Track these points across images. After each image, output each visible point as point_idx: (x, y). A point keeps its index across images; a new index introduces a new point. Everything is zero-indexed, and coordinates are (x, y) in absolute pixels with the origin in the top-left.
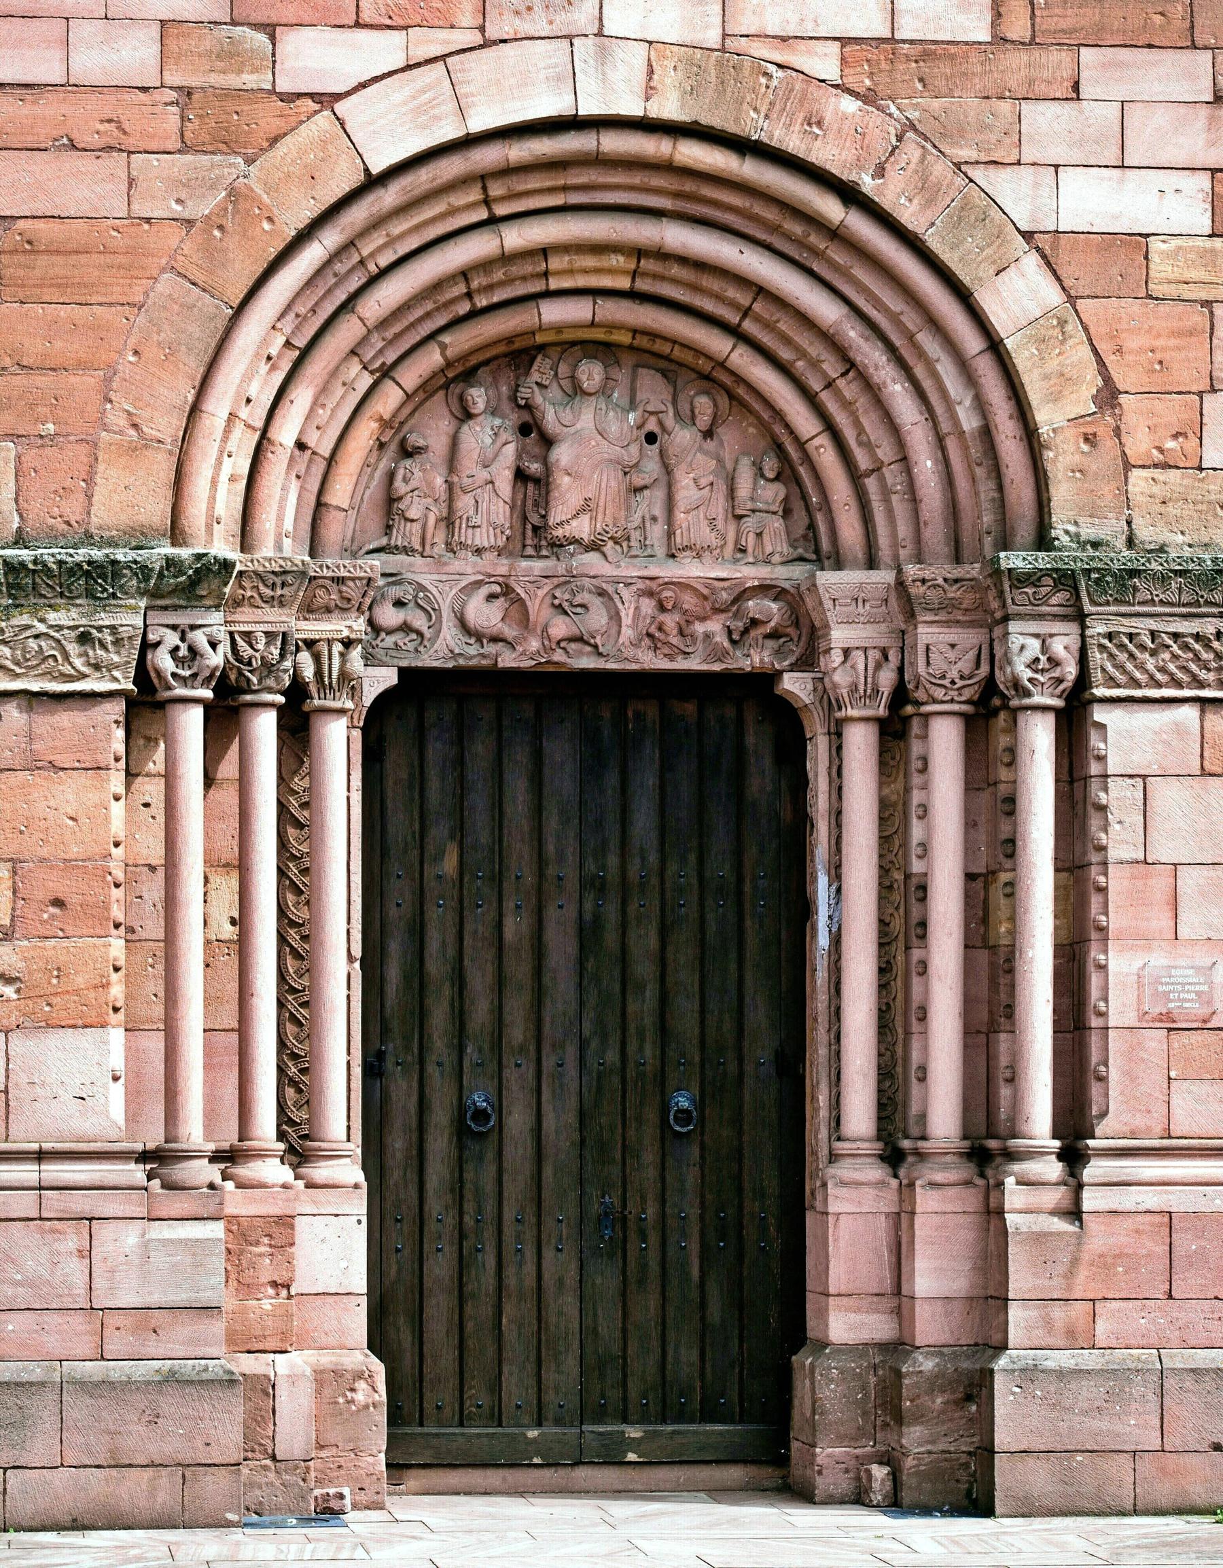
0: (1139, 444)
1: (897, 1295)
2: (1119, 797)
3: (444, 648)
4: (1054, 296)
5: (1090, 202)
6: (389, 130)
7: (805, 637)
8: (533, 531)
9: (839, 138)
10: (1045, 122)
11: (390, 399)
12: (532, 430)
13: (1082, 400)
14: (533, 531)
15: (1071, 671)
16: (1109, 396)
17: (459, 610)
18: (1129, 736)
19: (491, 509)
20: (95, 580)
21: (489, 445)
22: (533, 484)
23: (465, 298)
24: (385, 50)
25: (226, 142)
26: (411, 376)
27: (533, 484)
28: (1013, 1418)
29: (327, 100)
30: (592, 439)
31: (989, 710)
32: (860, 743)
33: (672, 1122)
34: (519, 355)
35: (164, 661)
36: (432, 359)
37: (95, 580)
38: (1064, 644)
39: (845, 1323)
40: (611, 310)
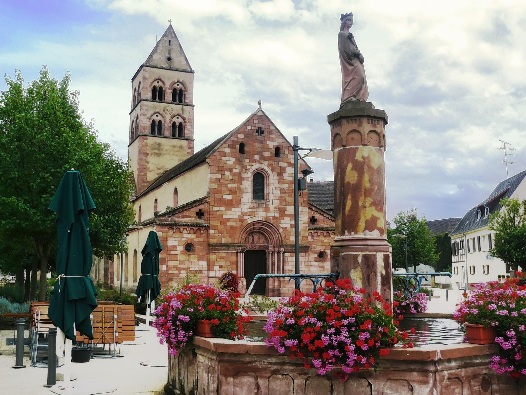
1: (274, 285)
2: (286, 258)
3: (248, 249)
5: (284, 226)
6: (250, 221)
7: (267, 248)
8: (253, 242)
9: (272, 221)
12: (253, 237)
14: (253, 242)
17: (249, 246)
18: (287, 254)
19: (251, 241)
20: (235, 246)
21: (251, 237)
22: (253, 240)
23: (250, 230)
24: (249, 217)
25: (241, 222)
27: (253, 240)
28: (282, 291)
30: (256, 237)
31: (279, 253)
32: (270, 255)
33: (257, 276)
34: (252, 233)
37: (235, 246)
39: (271, 287)
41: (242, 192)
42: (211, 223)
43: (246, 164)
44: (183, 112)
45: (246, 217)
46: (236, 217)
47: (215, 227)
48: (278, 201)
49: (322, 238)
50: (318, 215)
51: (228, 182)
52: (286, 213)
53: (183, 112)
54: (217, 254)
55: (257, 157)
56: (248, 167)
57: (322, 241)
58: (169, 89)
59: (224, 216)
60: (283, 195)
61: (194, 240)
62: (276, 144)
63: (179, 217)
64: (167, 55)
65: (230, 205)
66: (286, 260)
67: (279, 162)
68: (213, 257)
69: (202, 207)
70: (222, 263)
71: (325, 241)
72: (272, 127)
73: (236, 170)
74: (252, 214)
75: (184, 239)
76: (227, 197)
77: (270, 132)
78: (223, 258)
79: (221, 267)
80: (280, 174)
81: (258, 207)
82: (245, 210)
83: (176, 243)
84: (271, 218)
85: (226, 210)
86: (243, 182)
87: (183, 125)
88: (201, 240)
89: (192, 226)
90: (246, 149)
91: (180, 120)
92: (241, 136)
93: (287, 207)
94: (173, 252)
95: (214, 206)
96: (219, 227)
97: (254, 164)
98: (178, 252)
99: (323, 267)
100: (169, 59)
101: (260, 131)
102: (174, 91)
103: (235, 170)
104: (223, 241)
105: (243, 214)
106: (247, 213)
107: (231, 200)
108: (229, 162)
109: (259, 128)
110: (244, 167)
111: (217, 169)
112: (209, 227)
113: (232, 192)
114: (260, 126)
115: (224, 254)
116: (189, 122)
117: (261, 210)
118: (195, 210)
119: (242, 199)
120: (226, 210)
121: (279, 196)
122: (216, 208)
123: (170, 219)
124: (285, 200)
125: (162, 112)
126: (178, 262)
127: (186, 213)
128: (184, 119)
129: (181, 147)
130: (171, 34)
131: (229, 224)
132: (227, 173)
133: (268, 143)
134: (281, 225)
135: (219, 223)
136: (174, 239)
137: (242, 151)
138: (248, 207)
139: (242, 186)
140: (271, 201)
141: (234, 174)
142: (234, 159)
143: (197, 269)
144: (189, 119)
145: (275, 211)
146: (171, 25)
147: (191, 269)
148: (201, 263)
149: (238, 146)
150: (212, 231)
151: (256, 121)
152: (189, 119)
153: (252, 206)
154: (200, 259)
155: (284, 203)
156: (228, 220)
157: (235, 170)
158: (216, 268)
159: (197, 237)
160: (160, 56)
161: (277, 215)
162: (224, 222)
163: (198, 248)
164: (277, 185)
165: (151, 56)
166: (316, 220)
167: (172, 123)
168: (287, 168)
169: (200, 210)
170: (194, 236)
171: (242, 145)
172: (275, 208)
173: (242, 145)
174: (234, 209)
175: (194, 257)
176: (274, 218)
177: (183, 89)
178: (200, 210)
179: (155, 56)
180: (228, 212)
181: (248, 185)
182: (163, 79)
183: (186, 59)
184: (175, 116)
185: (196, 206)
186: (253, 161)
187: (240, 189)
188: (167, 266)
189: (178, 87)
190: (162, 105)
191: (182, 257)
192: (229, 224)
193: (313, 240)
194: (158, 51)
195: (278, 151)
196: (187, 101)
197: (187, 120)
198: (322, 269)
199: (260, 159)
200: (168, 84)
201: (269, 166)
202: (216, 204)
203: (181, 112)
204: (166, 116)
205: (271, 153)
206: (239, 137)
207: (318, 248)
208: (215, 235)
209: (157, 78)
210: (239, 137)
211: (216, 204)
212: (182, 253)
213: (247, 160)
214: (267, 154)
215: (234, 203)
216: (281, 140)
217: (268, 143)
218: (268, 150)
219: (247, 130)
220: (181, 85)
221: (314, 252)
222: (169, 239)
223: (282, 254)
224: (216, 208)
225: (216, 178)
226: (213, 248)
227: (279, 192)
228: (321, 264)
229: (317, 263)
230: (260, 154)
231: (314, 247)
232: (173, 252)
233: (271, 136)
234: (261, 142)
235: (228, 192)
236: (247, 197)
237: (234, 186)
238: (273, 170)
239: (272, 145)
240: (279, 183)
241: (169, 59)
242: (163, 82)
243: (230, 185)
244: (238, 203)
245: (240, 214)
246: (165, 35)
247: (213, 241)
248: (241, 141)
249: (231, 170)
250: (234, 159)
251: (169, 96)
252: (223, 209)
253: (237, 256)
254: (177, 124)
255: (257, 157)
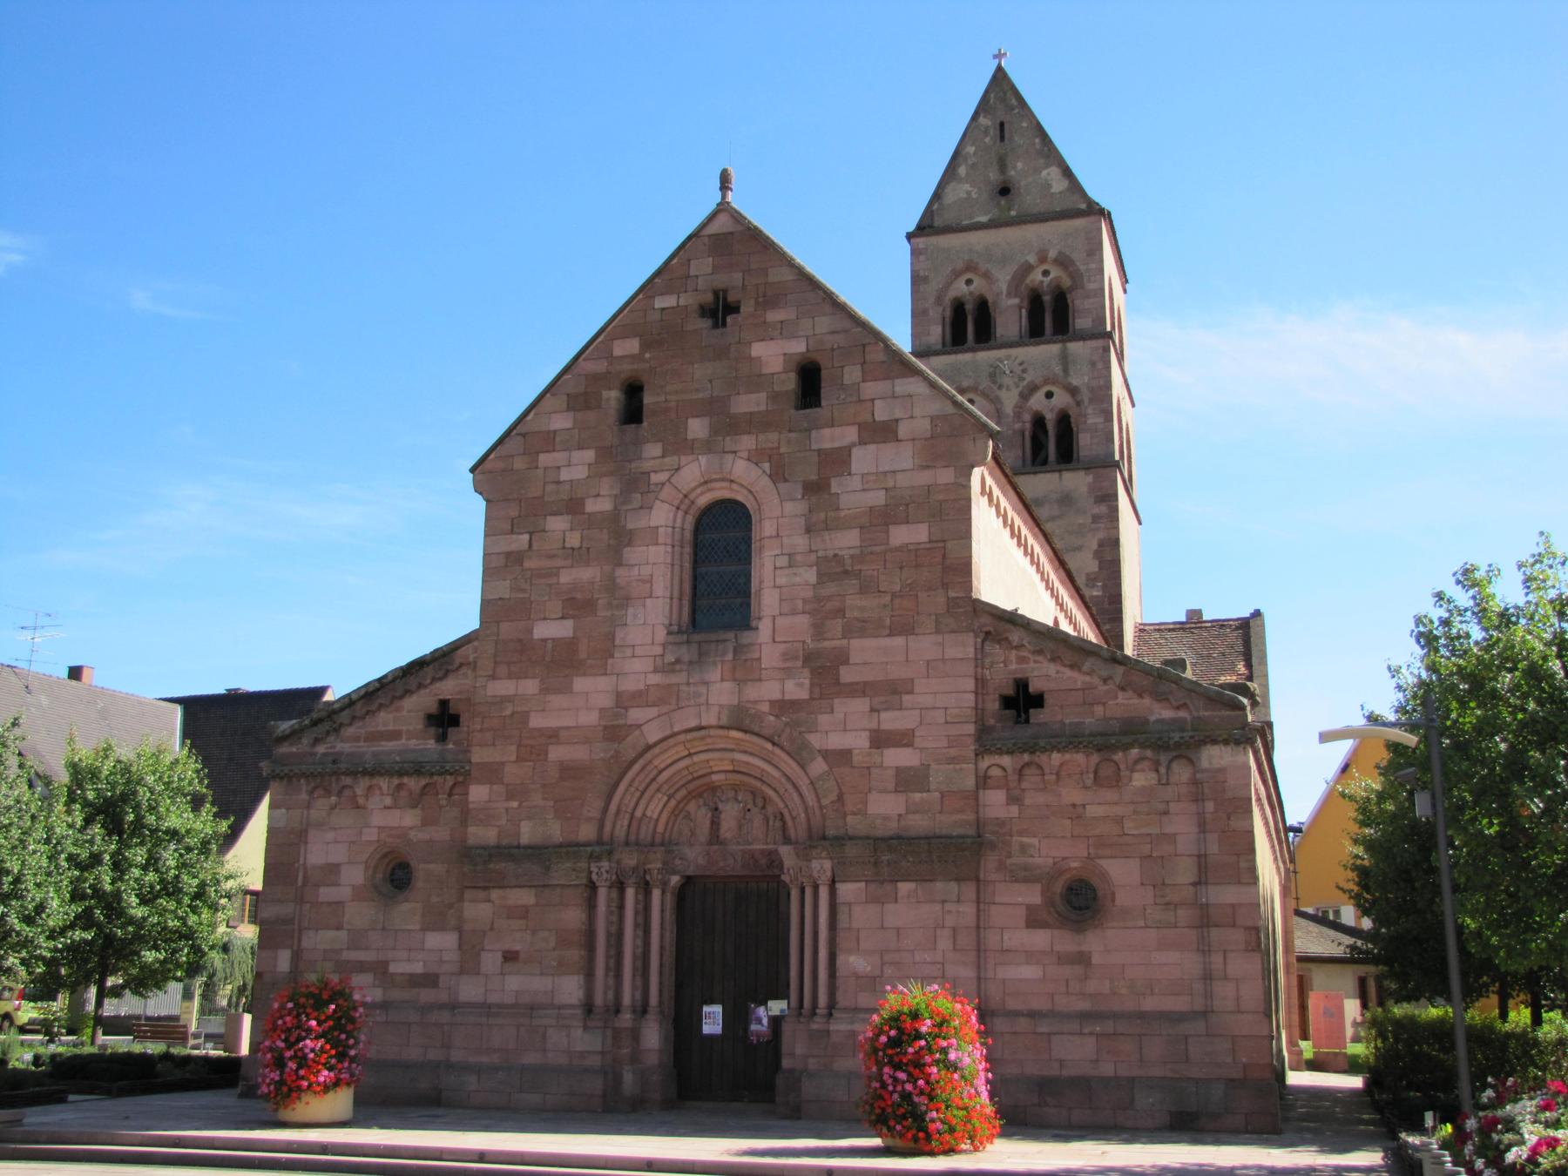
0: (849, 807)
4: (826, 768)
5: (836, 741)
8: (715, 837)
10: (823, 719)
11: (673, 803)
13: (833, 797)
14: (715, 837)
15: (829, 874)
16: (840, 797)
22: (715, 824)
24: (653, 712)
26: (679, 796)
27: (715, 824)
29: (639, 726)
35: (594, 877)
36: (683, 792)
38: (828, 864)
40: (730, 776)
41: (621, 599)
42: (479, 755)
43: (647, 465)
44: (1066, 370)
45: (636, 715)
46: (590, 718)
47: (492, 773)
48: (803, 621)
49: (1071, 794)
50: (1051, 669)
51: (558, 563)
52: (847, 675)
53: (1066, 370)
54: (495, 894)
55: (697, 428)
56: (655, 478)
57: (1076, 813)
58: (1009, 295)
59: (536, 721)
60: (830, 589)
61: (413, 835)
62: (798, 347)
63: (357, 739)
64: (994, 176)
65: (562, 663)
66: (842, 917)
67: (816, 426)
68: (477, 911)
69: (448, 688)
70: (517, 941)
71: (1093, 811)
72: (779, 275)
73: (599, 505)
74: (666, 698)
75: (370, 835)
76: (552, 629)
77: (770, 300)
78: (523, 913)
79: (510, 957)
80: (816, 489)
81: (700, 661)
82: (630, 685)
83: (338, 854)
84: (765, 708)
85: (545, 690)
86: (633, 554)
87: (1073, 413)
88: (441, 833)
89: (400, 774)
90: (648, 399)
91: (1061, 399)
92: (630, 346)
93: (856, 643)
94: (326, 894)
95: (493, 677)
96: (512, 773)
97: (684, 460)
98: (343, 892)
99: (1082, 959)
100: (1005, 191)
101: (720, 310)
102: (1035, 303)
103: (592, 506)
104: (528, 833)
105: (623, 701)
106: (640, 698)
107: (570, 644)
108: (565, 475)
109: (716, 293)
110: (635, 486)
111: (514, 513)
112: (468, 774)
113: (577, 605)
114: (721, 281)
115: (526, 897)
116: (1091, 400)
117: (714, 674)
118: (421, 702)
119: (620, 634)
120: (545, 690)
121: (809, 594)
122: (503, 687)
123: (321, 749)
124: (840, 612)
125: (985, 384)
126: (343, 934)
127: (384, 720)
128: (1073, 391)
129: (1066, 500)
130: (1003, 100)
131: (556, 753)
132: (557, 524)
133: (757, 349)
134: (815, 740)
135: (511, 753)
136: (330, 836)
137: (633, 413)
138: (648, 665)
139: (620, 572)
140: (764, 627)
141: (592, 521)
142: (589, 455)
143: (418, 968)
144: (1092, 390)
145: (787, 672)
146: (999, 69)
147: (393, 968)
148: (435, 940)
149: (613, 397)
150: (478, 793)
151: (702, 267)
152: (1092, 390)
153: (670, 658)
154: (435, 922)
155: (836, 626)
156: (553, 735)
157: (592, 506)
158: (491, 960)
159: (426, 822)
160: (967, 187)
161: (797, 689)
162: (535, 746)
163: (426, 871)
164: (800, 542)
165: (937, 195)
166: (1038, 701)
167: (1027, 417)
168: (855, 452)
169: (444, 703)
170: (408, 819)
171: (633, 391)
172: (786, 656)
173: (633, 391)
174: (580, 684)
175: (407, 913)
176: (782, 706)
177: (1066, 282)
178: (444, 703)
179: (951, 195)
180: (556, 700)
181: (656, 566)
182: (983, 267)
183: (1067, 172)
184: (1033, 389)
185: (420, 686)
186: (680, 446)
187: (611, 586)
188: (297, 956)
189: (1047, 280)
190: (985, 356)
191: (360, 914)
192: (556, 753)
193: (1014, 810)
194: (962, 171)
195: (810, 382)
196: (1081, 323)
197: (1085, 396)
198: (1079, 969)
199: (715, 431)
200: (1003, 278)
201: (755, 458)
202: (502, 670)
203: (1058, 369)
204: (1003, 394)
205: (774, 397)
206: (617, 352)
207: (1053, 849)
208: (493, 810)
209: (960, 265)
210: (617, 352)
211: (502, 670)
212: (358, 894)
213: (653, 450)
214: (749, 403)
215: (583, 655)
216: (825, 323)
217: (757, 349)
218: (757, 381)
219: (657, 316)
220: (1055, 272)
221: (1025, 876)
222: (312, 833)
223: (824, 893)
224: (503, 687)
225: (508, 554)
226: (484, 865)
227: (811, 576)
228: (1066, 941)
229: (1040, 939)
230: (714, 408)
231: (1024, 849)
232: (326, 894)
233: (773, 316)
234: (721, 353)
235: (555, 607)
236: (650, 619)
237: (587, 574)
238: (778, 475)
239: (774, 355)
240: (808, 530)
241: (1005, 191)
242: (987, 275)
243: (565, 578)
244: (606, 652)
245: (607, 701)
246: (983, 107)
247: (482, 834)
248: (627, 369)
249: (573, 506)
250: (589, 455)
251: (1010, 319)
252: (530, 686)
253: (591, 905)
254: (1050, 417)
255: (697, 428)
